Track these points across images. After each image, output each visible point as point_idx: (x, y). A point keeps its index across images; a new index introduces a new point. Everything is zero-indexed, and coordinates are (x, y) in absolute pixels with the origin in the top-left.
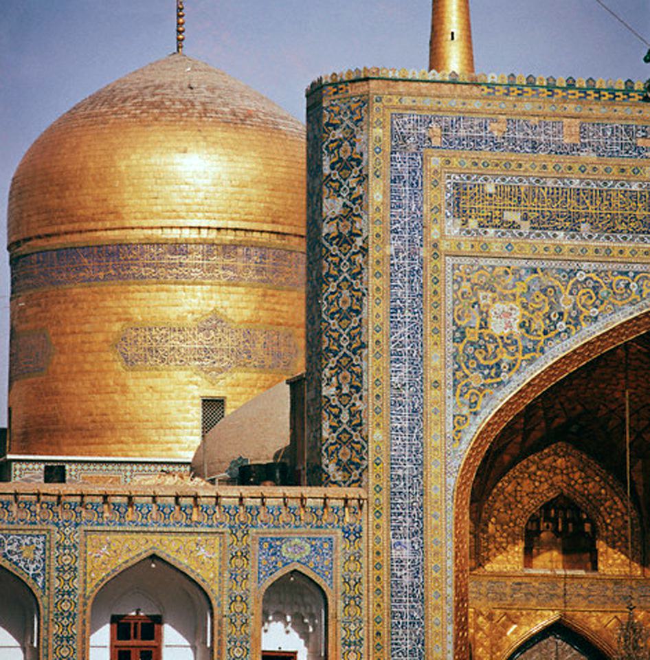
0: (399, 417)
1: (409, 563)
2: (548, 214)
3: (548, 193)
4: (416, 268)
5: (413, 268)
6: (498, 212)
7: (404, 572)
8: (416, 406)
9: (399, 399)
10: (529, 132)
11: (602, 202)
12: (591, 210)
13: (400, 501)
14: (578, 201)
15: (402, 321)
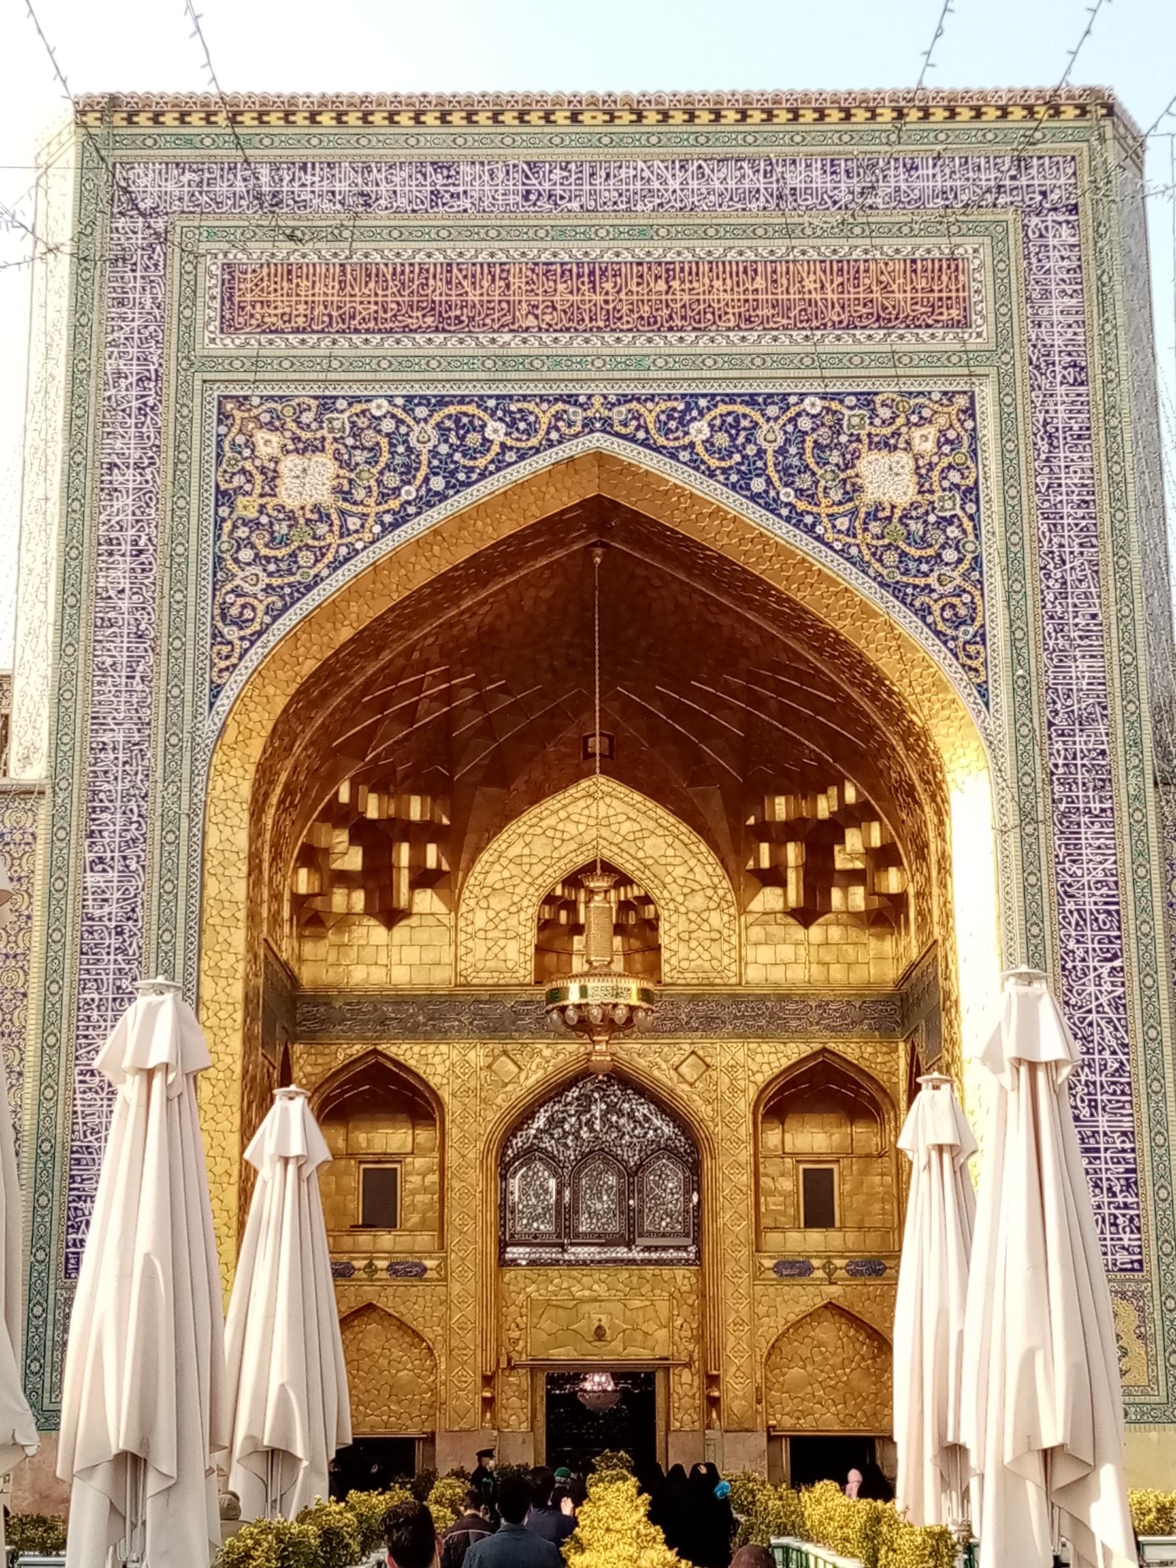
0: (111, 646)
1: (117, 895)
2: (394, 306)
3: (394, 274)
4: (150, 403)
5: (145, 404)
6: (302, 307)
7: (107, 909)
8: (142, 627)
9: (112, 615)
11: (493, 281)
12: (473, 297)
13: (106, 787)
14: (449, 282)
15: (120, 487)
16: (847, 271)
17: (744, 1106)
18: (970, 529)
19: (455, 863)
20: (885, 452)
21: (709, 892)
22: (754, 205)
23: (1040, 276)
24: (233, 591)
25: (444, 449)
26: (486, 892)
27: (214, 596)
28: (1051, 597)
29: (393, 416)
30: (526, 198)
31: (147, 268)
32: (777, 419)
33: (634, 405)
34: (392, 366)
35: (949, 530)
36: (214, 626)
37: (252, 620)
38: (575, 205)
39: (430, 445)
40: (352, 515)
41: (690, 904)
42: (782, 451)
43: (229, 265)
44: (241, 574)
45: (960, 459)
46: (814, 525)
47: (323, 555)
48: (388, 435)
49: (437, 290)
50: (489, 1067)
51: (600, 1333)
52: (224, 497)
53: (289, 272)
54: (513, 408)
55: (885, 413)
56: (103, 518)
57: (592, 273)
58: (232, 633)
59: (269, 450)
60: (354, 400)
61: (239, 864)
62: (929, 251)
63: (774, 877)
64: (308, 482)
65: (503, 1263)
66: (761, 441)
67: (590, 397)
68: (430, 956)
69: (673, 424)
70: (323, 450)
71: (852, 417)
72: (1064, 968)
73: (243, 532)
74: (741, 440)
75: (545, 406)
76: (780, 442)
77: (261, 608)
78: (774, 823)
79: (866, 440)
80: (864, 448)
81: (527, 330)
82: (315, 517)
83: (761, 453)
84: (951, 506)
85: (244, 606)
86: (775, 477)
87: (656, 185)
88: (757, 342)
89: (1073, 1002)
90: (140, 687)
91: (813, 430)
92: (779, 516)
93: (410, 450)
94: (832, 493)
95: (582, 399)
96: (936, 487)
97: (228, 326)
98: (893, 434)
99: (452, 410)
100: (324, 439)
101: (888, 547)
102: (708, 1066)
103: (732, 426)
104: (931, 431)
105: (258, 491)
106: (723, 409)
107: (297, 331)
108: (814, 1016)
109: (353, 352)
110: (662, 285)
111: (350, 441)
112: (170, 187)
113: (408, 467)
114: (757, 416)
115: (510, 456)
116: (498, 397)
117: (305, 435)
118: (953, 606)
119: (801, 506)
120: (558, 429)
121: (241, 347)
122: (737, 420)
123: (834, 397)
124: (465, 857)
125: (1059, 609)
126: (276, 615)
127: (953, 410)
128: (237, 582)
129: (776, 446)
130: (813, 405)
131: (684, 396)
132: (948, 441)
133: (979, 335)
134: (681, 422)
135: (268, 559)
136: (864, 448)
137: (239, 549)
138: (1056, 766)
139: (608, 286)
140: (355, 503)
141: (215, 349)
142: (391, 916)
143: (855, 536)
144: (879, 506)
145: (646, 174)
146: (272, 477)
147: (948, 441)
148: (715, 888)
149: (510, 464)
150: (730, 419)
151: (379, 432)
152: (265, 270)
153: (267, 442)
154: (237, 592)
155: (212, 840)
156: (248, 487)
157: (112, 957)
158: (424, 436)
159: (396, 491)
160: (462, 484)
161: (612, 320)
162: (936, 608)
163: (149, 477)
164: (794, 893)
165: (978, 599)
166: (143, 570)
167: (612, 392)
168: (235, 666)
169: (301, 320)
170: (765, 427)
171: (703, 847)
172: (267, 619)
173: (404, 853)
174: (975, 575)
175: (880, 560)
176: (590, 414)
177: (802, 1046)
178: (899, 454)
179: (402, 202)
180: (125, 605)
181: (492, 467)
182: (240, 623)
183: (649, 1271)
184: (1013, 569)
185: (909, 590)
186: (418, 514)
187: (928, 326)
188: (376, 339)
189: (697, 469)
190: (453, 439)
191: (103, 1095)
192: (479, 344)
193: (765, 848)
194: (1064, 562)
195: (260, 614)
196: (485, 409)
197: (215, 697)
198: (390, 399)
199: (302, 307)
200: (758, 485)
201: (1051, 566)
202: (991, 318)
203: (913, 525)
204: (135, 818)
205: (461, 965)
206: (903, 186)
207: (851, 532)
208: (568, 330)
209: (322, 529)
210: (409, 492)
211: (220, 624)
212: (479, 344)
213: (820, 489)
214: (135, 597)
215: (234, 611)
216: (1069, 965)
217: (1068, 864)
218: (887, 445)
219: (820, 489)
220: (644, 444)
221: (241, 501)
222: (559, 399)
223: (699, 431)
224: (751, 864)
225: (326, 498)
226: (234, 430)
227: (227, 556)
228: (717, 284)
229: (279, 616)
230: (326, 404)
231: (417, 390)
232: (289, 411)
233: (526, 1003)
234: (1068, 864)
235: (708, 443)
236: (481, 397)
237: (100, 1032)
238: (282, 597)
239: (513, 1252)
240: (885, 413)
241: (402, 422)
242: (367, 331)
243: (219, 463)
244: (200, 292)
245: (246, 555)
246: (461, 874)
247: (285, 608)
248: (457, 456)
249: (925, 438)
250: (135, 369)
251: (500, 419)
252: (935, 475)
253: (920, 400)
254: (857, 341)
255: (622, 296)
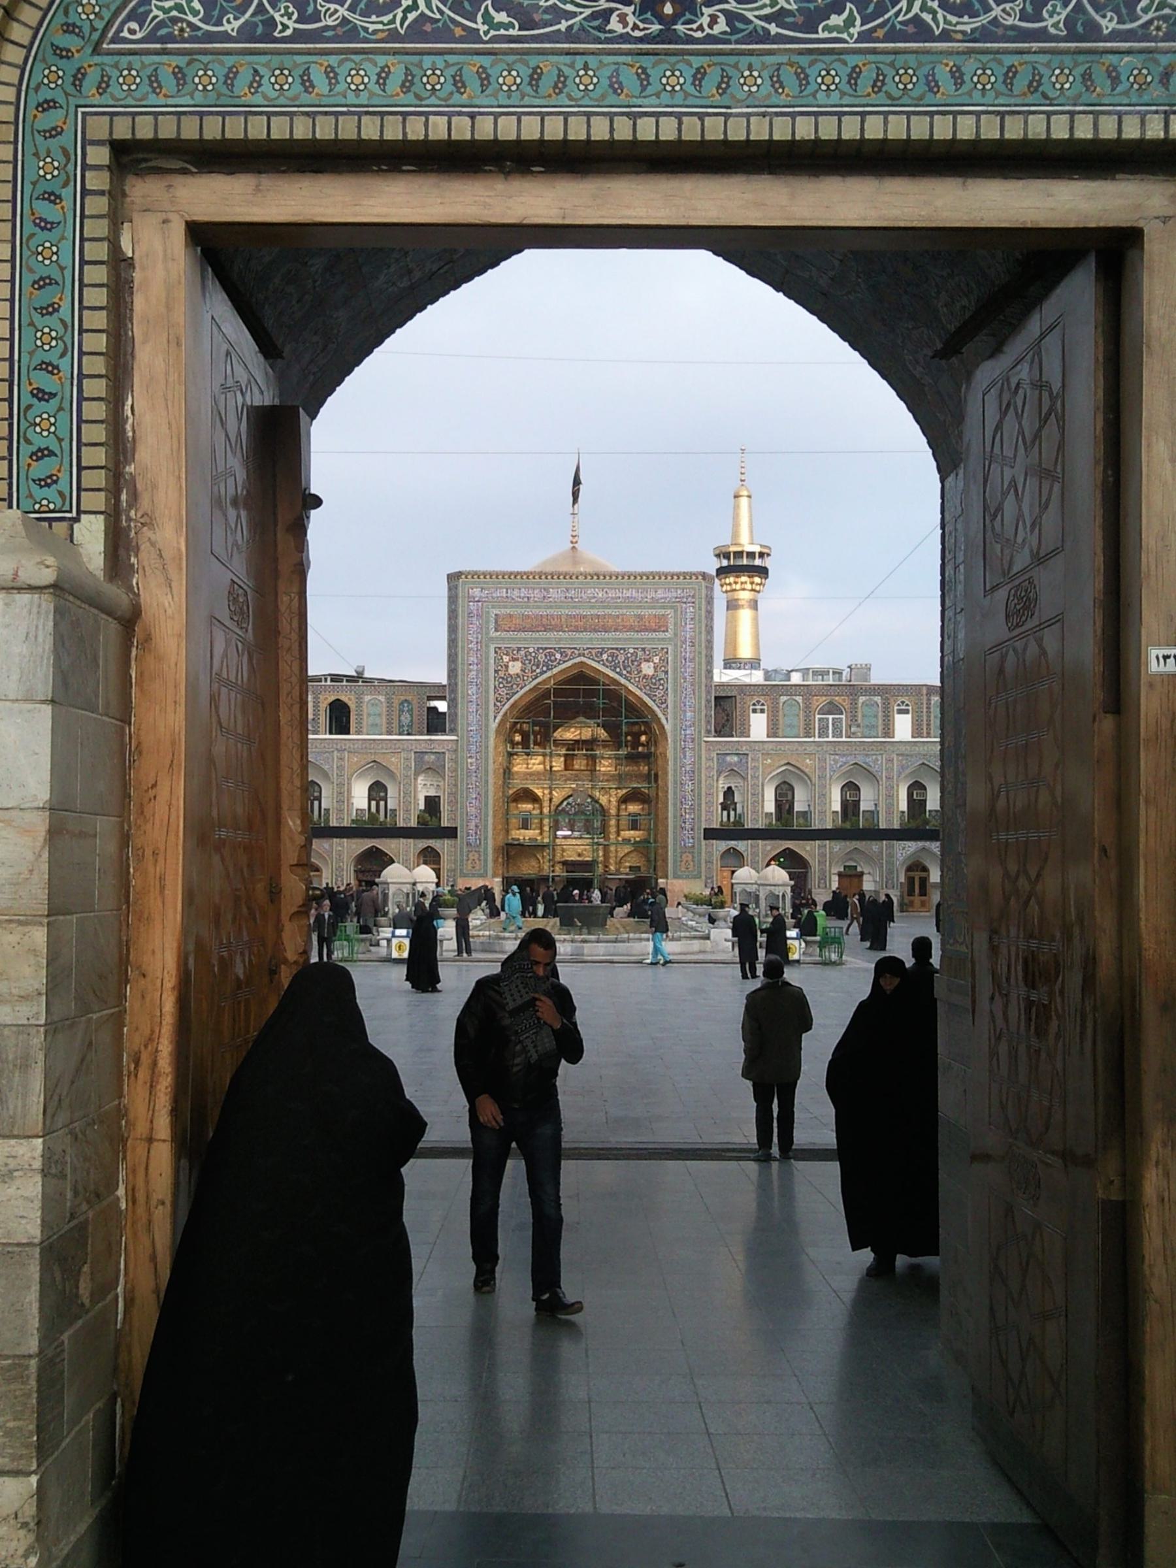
16: (640, 617)
34: (532, 641)
52: (496, 671)
71: (640, 653)
97: (496, 630)
103: (612, 655)
130: (631, 651)
158: (541, 657)
218: (648, 661)
223: (605, 656)
230: (519, 649)
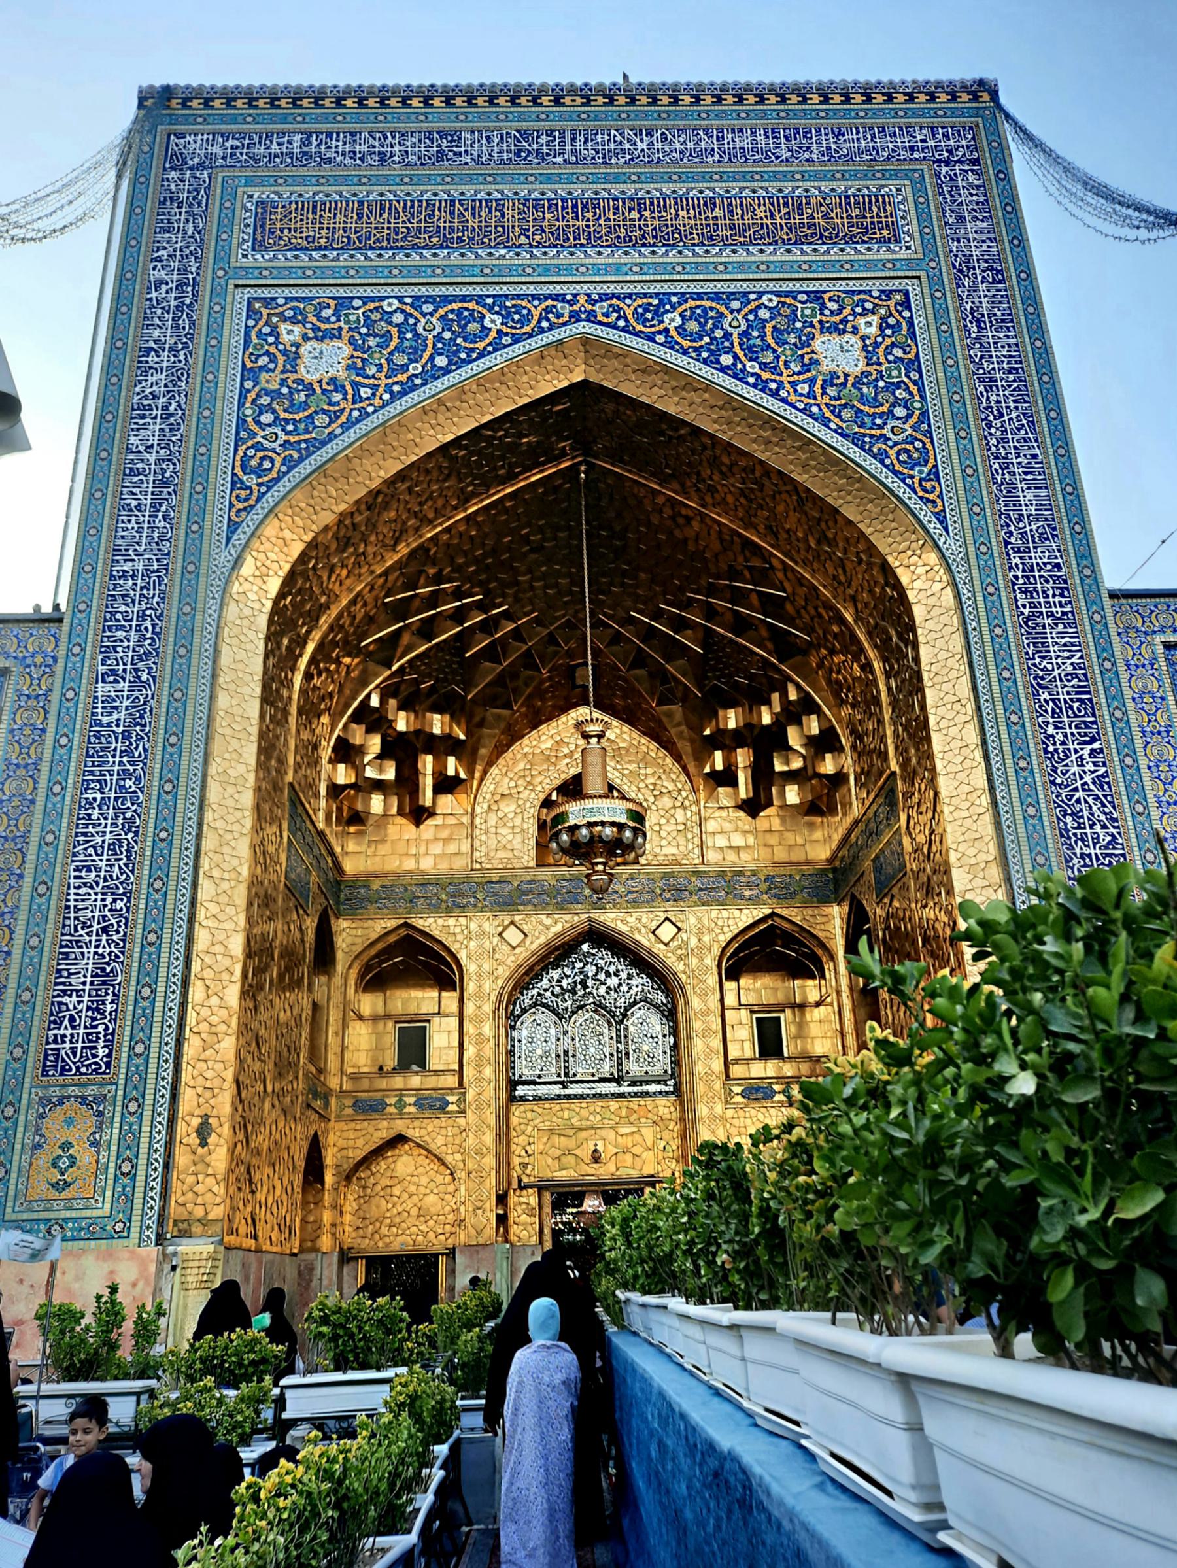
1: (126, 703)
3: (405, 207)
4: (188, 301)
7: (115, 716)
8: (168, 475)
9: (140, 465)
10: (377, 144)
13: (123, 608)
14: (452, 213)
17: (710, 961)
18: (915, 392)
19: (471, 772)
20: (835, 335)
21: (675, 794)
22: (710, 160)
23: (954, 207)
24: (252, 447)
25: (447, 335)
26: (497, 797)
27: (236, 450)
28: (994, 441)
29: (403, 311)
30: (518, 154)
31: (191, 205)
32: (739, 311)
33: (614, 301)
35: (897, 393)
36: (234, 474)
37: (270, 470)
38: (559, 159)
39: (435, 333)
40: (365, 386)
41: (659, 804)
42: (745, 334)
43: (263, 202)
44: (262, 433)
45: (901, 339)
46: (778, 390)
47: (338, 417)
48: (397, 325)
49: (441, 219)
50: (500, 934)
51: (596, 1157)
53: (315, 207)
54: (508, 304)
55: (833, 306)
56: (137, 389)
57: (575, 206)
58: (252, 480)
59: (292, 338)
60: (366, 300)
61: (252, 685)
62: (859, 190)
63: (727, 778)
64: (326, 361)
65: (512, 1099)
66: (726, 326)
67: (575, 295)
68: (452, 848)
69: (649, 315)
70: (340, 337)
71: (806, 310)
72: (1046, 751)
73: (266, 400)
74: (709, 325)
75: (536, 303)
76: (743, 327)
77: (278, 460)
78: (726, 731)
79: (818, 326)
80: (817, 332)
81: (520, 246)
82: (331, 388)
83: (727, 336)
84: (898, 375)
85: (263, 458)
86: (741, 354)
87: (627, 146)
88: (721, 255)
89: (1059, 781)
90: (162, 524)
91: (772, 319)
92: (747, 383)
93: (417, 335)
94: (792, 365)
95: (569, 297)
96: (882, 359)
98: (841, 321)
99: (455, 306)
100: (340, 328)
101: (845, 406)
102: (679, 929)
104: (875, 319)
105: (280, 367)
106: (691, 303)
107: (320, 248)
108: (764, 887)
109: (369, 263)
110: (635, 215)
111: (364, 330)
112: (217, 150)
113: (416, 349)
114: (722, 309)
115: (506, 340)
116: (494, 296)
117: (323, 326)
118: (907, 451)
119: (765, 375)
120: (548, 320)
121: (270, 260)
122: (705, 311)
123: (787, 294)
124: (479, 768)
125: (1002, 451)
126: (291, 464)
127: (892, 303)
128: (259, 439)
129: (740, 330)
131: (657, 294)
132: (889, 326)
133: (908, 248)
134: (656, 313)
135: (287, 421)
136: (817, 332)
137: (261, 413)
138: (1016, 577)
139: (589, 215)
140: (368, 377)
141: (248, 262)
142: (419, 815)
143: (815, 398)
144: (834, 375)
145: (619, 138)
146: (293, 358)
147: (889, 326)
148: (679, 791)
149: (506, 346)
150: (699, 311)
151: (390, 323)
152: (294, 206)
153: (289, 332)
154: (258, 447)
155: (224, 661)
156: (271, 366)
157: (117, 759)
158: (430, 326)
159: (404, 368)
160: (463, 361)
161: (594, 240)
162: (892, 453)
163: (182, 358)
164: (744, 790)
165: (929, 445)
166: (171, 430)
167: (596, 291)
168: (252, 507)
169: (323, 241)
170: (730, 317)
171: (669, 760)
172: (284, 469)
173: (427, 763)
174: (925, 427)
175: (839, 416)
176: (575, 308)
177: (755, 912)
178: (847, 337)
179: (413, 158)
180: (152, 458)
181: (490, 348)
182: (259, 471)
183: (635, 1103)
184: (959, 419)
185: (867, 439)
186: (423, 385)
187: (864, 242)
188: (388, 254)
189: (672, 348)
190: (455, 328)
191: (98, 890)
192: (477, 256)
193: (718, 755)
194: (1002, 415)
195: (277, 465)
196: (484, 306)
197: (233, 532)
198: (400, 299)
199: (324, 232)
200: (726, 360)
201: (991, 418)
202: (917, 236)
203: (865, 390)
204: (149, 635)
205: (476, 854)
206: (833, 146)
207: (811, 395)
208: (555, 246)
209: (337, 397)
210: (416, 368)
211: (240, 473)
212: (477, 256)
213: (781, 363)
214: (162, 452)
215: (253, 463)
216: (1051, 749)
217: (1037, 661)
218: (838, 329)
219: (781, 363)
220: (624, 330)
221: (264, 376)
222: (548, 297)
223: (672, 320)
224: (707, 769)
225: (342, 374)
226: (261, 323)
227: (249, 419)
228: (682, 213)
229: (295, 466)
230: (343, 303)
231: (424, 291)
232: (310, 309)
233: (530, 882)
234: (1037, 661)
235: (680, 329)
236: (480, 296)
237: (99, 829)
238: (299, 451)
239: (521, 1091)
240: (833, 306)
241: (411, 315)
242: (381, 248)
243: (246, 348)
244: (237, 221)
245: (267, 418)
246: (475, 783)
247: (301, 459)
248: (459, 341)
249: (869, 324)
250: (175, 277)
251: (497, 313)
252: (881, 351)
253: (862, 296)
254: (803, 252)
255: (601, 222)
